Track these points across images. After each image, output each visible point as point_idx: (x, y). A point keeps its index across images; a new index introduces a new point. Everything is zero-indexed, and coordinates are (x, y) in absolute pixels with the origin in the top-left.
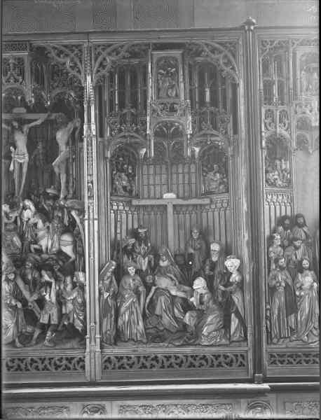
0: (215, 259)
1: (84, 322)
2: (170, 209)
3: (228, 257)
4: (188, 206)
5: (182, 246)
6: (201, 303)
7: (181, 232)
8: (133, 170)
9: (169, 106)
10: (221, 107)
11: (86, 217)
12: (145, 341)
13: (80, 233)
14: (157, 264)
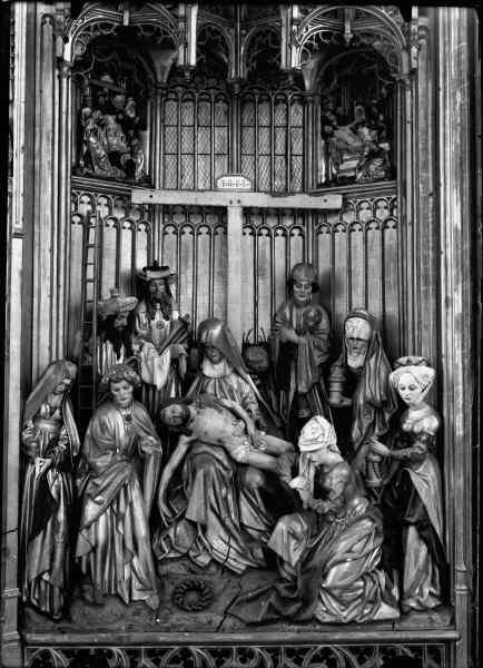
0: (355, 361)
2: (235, 221)
3: (403, 360)
5: (265, 323)
6: (321, 492)
8: (140, 109)
12: (153, 602)
14: (195, 370)
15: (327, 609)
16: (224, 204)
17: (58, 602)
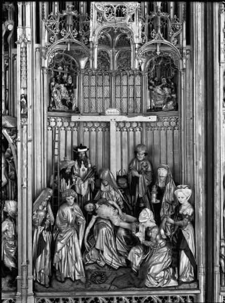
0: (161, 185)
1: (15, 260)
2: (113, 127)
3: (179, 186)
4: (131, 123)
5: (125, 167)
6: (147, 238)
7: (124, 150)
8: (74, 80)
9: (115, 9)
10: (172, 11)
11: (19, 137)
13: (12, 155)
14: (98, 188)
15: (151, 282)
16: (108, 120)
17: (48, 281)
